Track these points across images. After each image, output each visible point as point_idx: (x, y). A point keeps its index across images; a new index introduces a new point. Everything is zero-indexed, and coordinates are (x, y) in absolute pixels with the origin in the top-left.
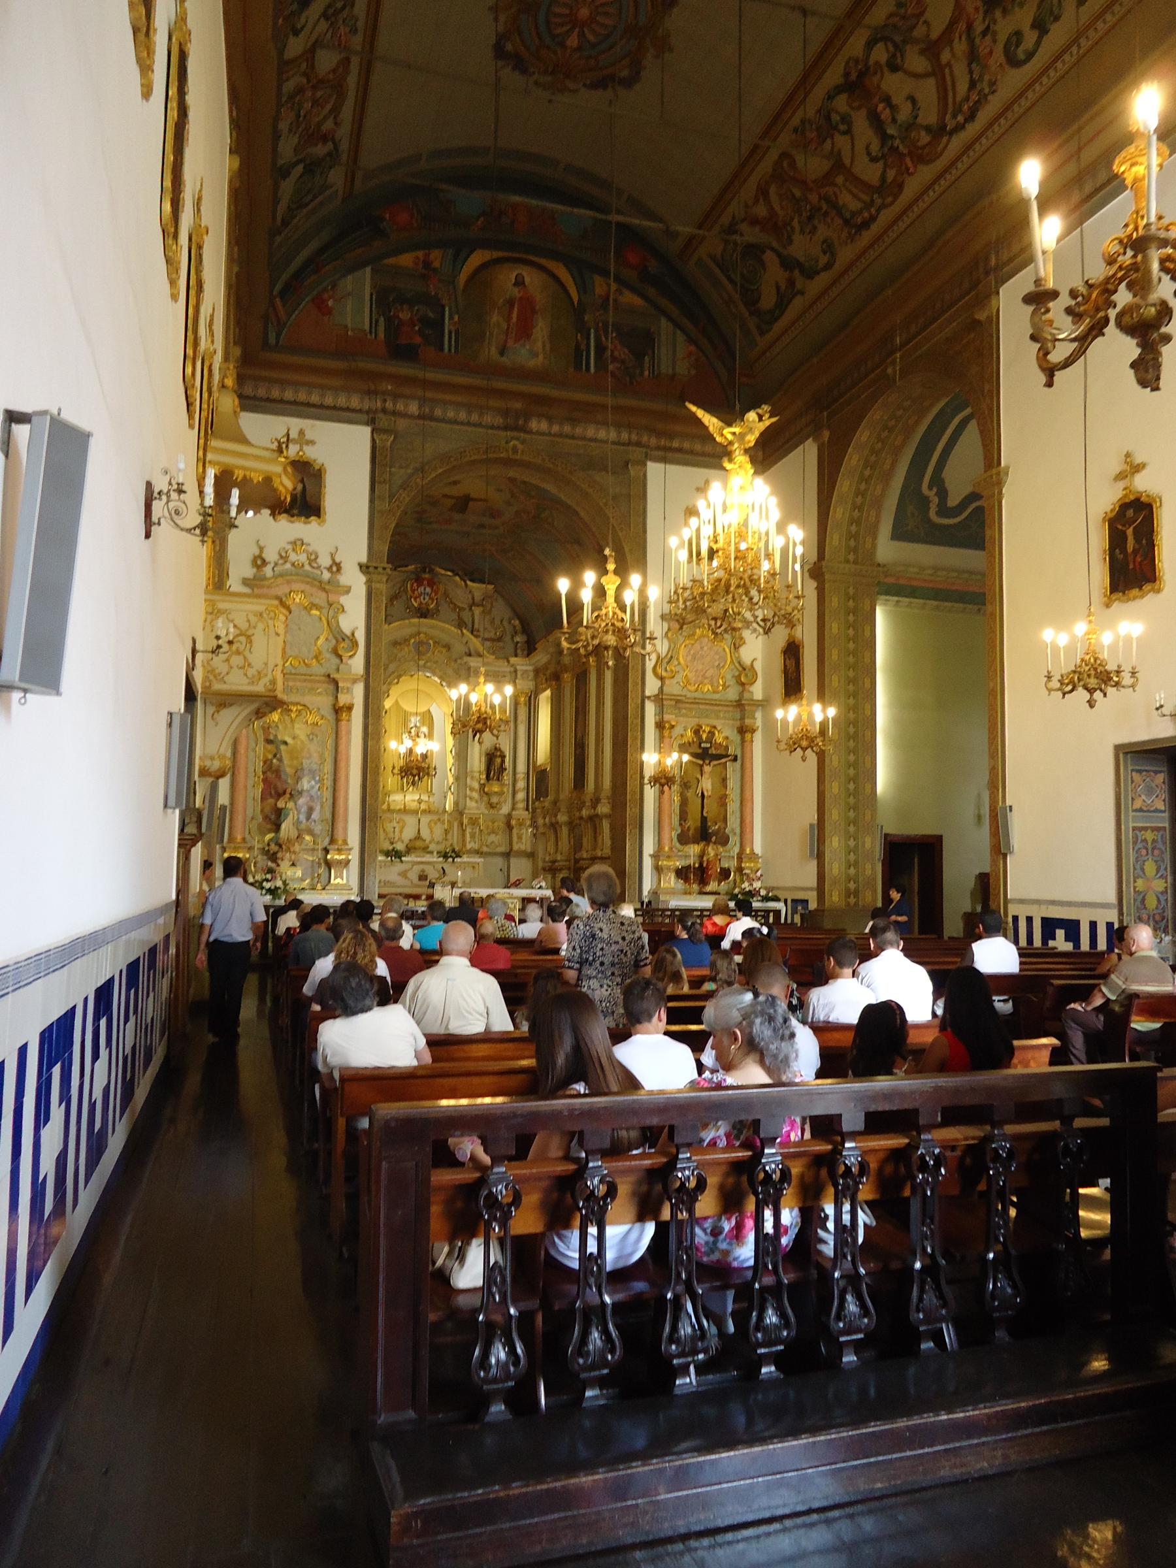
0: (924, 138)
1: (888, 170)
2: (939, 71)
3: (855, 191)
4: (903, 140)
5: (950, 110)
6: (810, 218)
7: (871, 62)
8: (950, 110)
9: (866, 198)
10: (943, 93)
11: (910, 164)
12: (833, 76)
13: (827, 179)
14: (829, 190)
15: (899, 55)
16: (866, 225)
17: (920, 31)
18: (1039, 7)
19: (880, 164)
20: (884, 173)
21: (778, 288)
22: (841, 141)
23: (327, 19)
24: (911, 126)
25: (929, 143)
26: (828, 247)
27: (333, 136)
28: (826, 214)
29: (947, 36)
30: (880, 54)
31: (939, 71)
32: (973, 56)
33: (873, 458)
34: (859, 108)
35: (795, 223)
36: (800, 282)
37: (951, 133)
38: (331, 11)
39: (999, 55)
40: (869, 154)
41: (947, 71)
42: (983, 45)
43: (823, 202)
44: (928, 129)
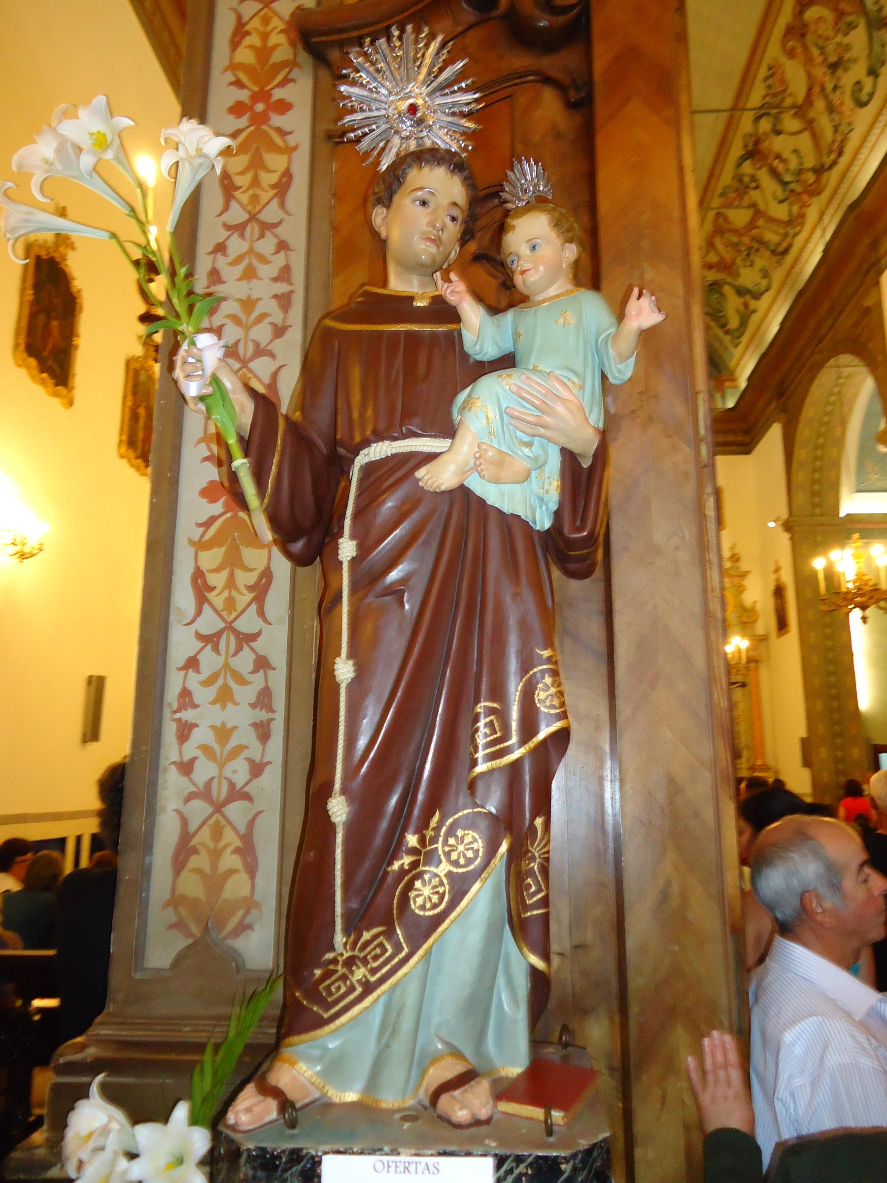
0: (811, 177)
2: (810, 126)
6: (748, 255)
9: (782, 231)
12: (737, 150)
13: (752, 225)
16: (786, 251)
17: (788, 102)
20: (790, 211)
21: (738, 311)
22: (755, 195)
24: (800, 171)
25: (815, 182)
26: (765, 274)
28: (757, 250)
29: (809, 100)
30: (765, 125)
31: (810, 126)
32: (831, 109)
33: (823, 429)
34: (760, 168)
35: (739, 261)
36: (753, 304)
39: (849, 103)
40: (776, 199)
42: (836, 98)
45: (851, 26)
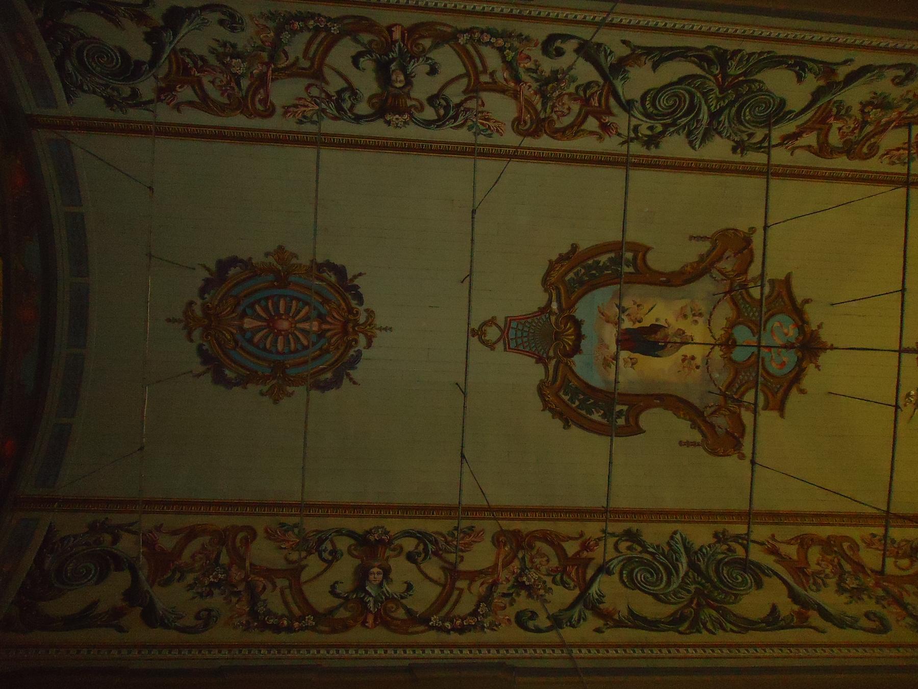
0: (401, 614)
1: (342, 609)
3: (289, 598)
4: (375, 602)
5: (442, 613)
6: (217, 585)
7: (396, 542)
8: (442, 613)
9: (296, 611)
10: (442, 601)
11: (370, 619)
13: (270, 573)
14: (261, 581)
15: (423, 555)
18: (560, 611)
19: (337, 602)
21: (95, 604)
22: (314, 564)
23: (339, 93)
24: (395, 600)
25: (403, 621)
26: (207, 619)
27: (162, 101)
30: (409, 544)
32: (486, 599)
34: (356, 557)
35: (190, 578)
37: (432, 628)
38: (347, 95)
39: (511, 612)
40: (333, 587)
41: (456, 593)
43: (244, 583)
44: (409, 611)
45: (564, 584)
